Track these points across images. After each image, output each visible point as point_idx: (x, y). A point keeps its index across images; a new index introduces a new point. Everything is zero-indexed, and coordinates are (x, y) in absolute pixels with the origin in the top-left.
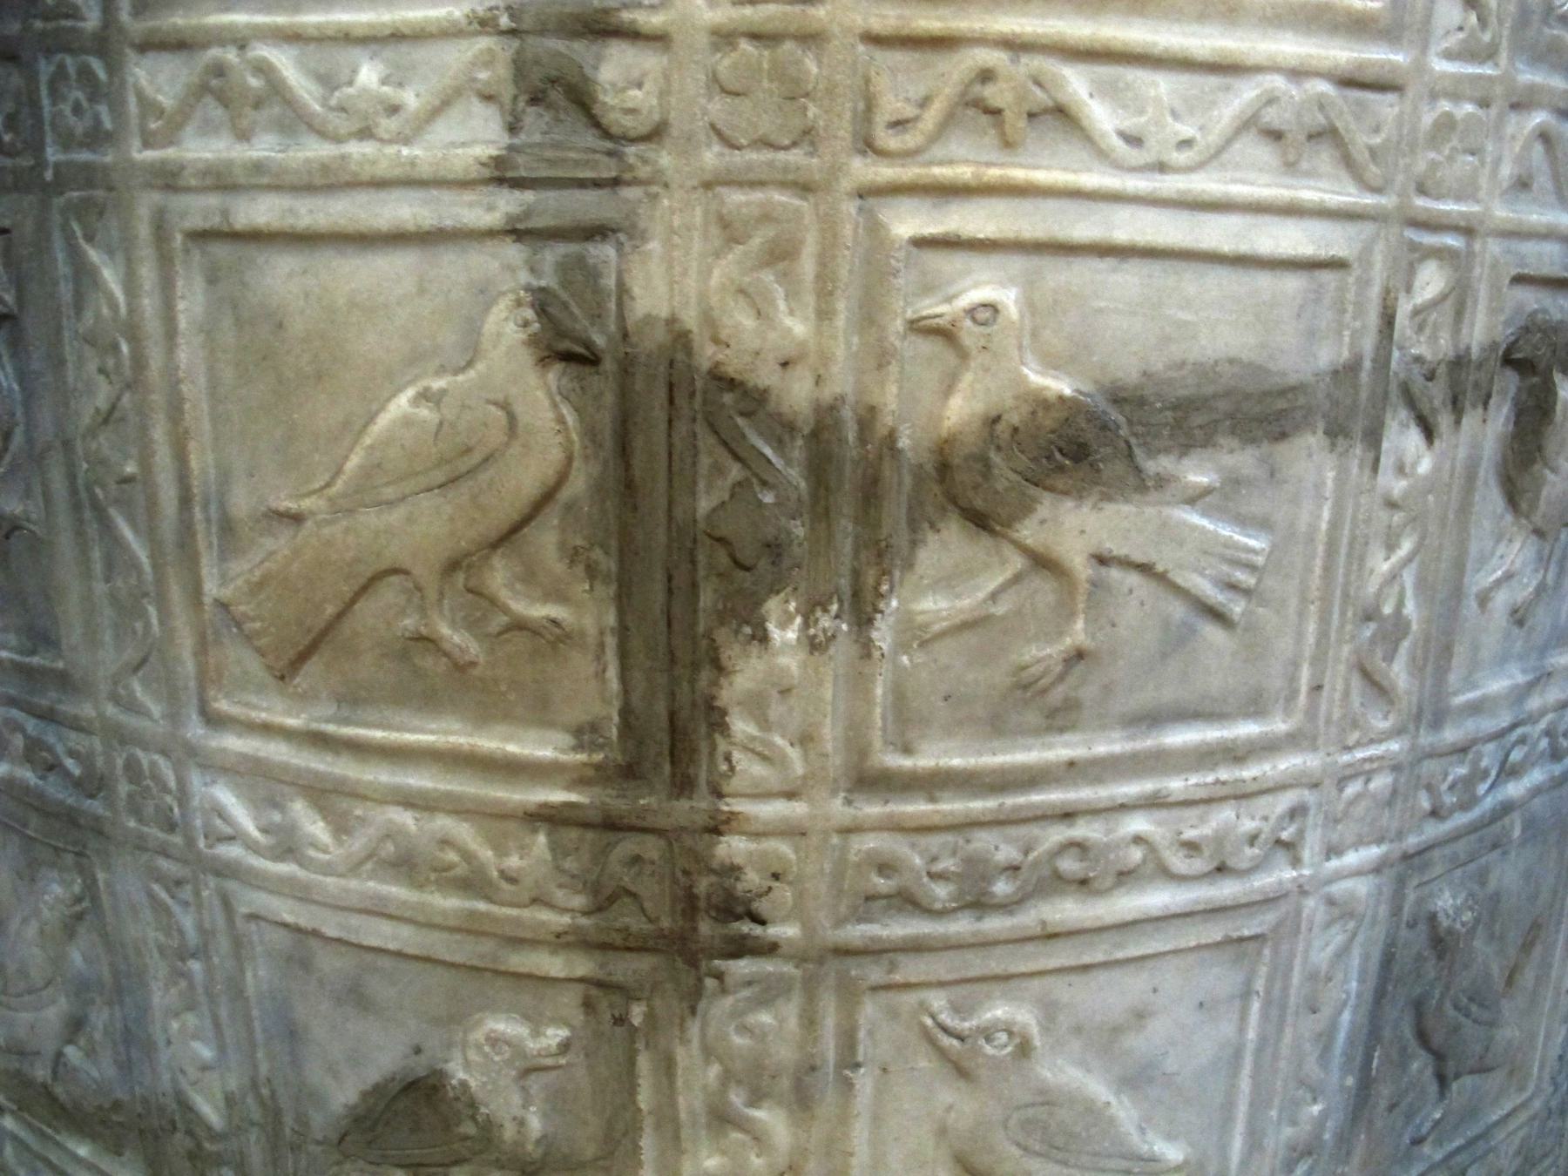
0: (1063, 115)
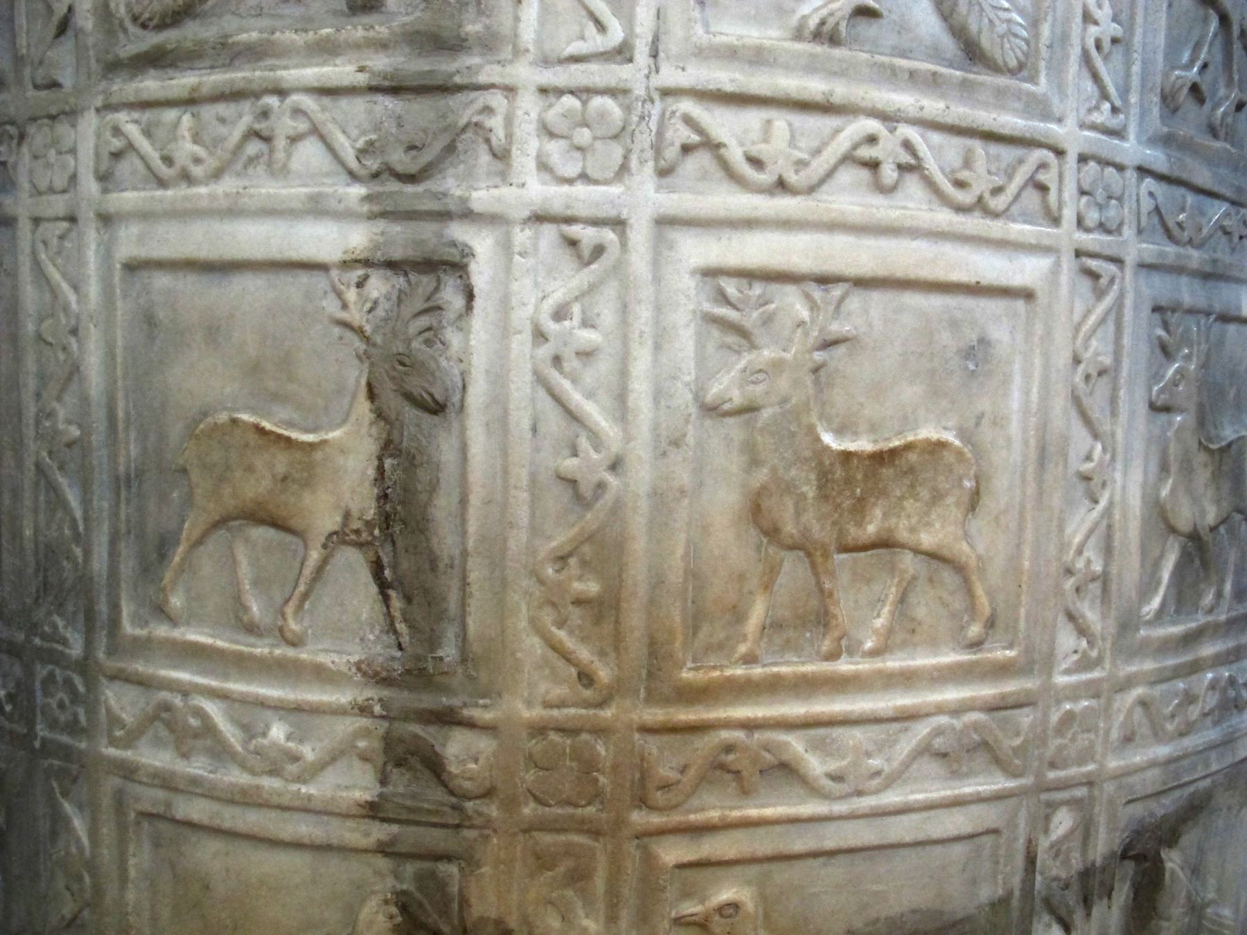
0: (787, 770)
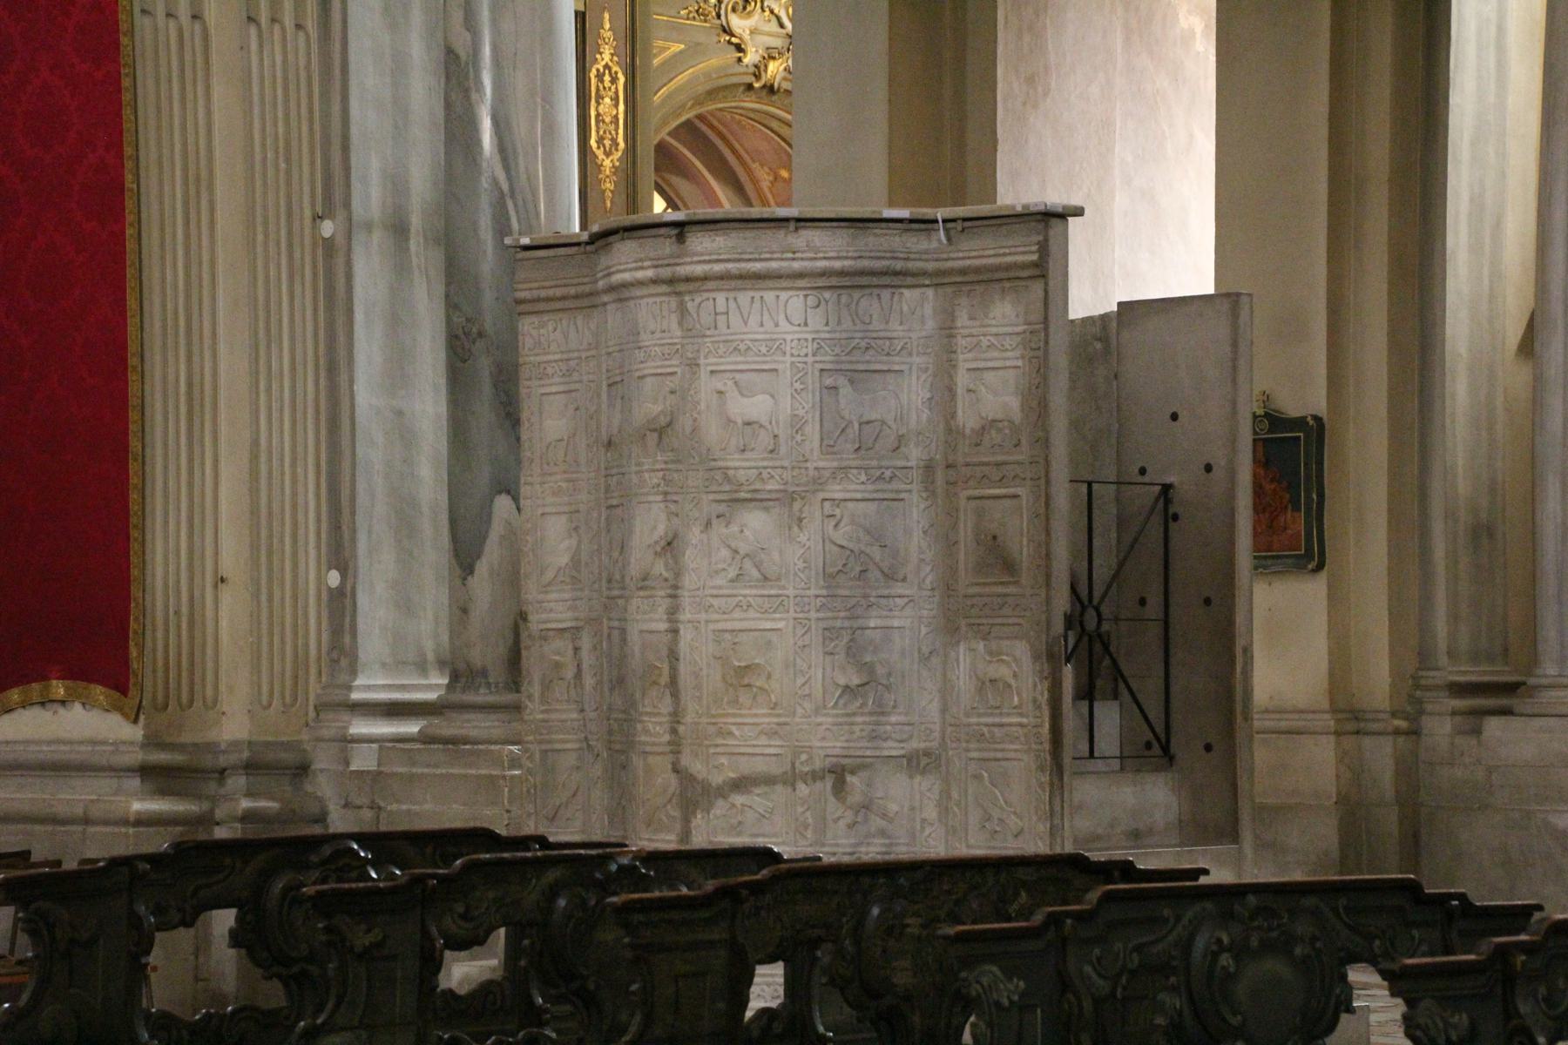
0: (730, 733)
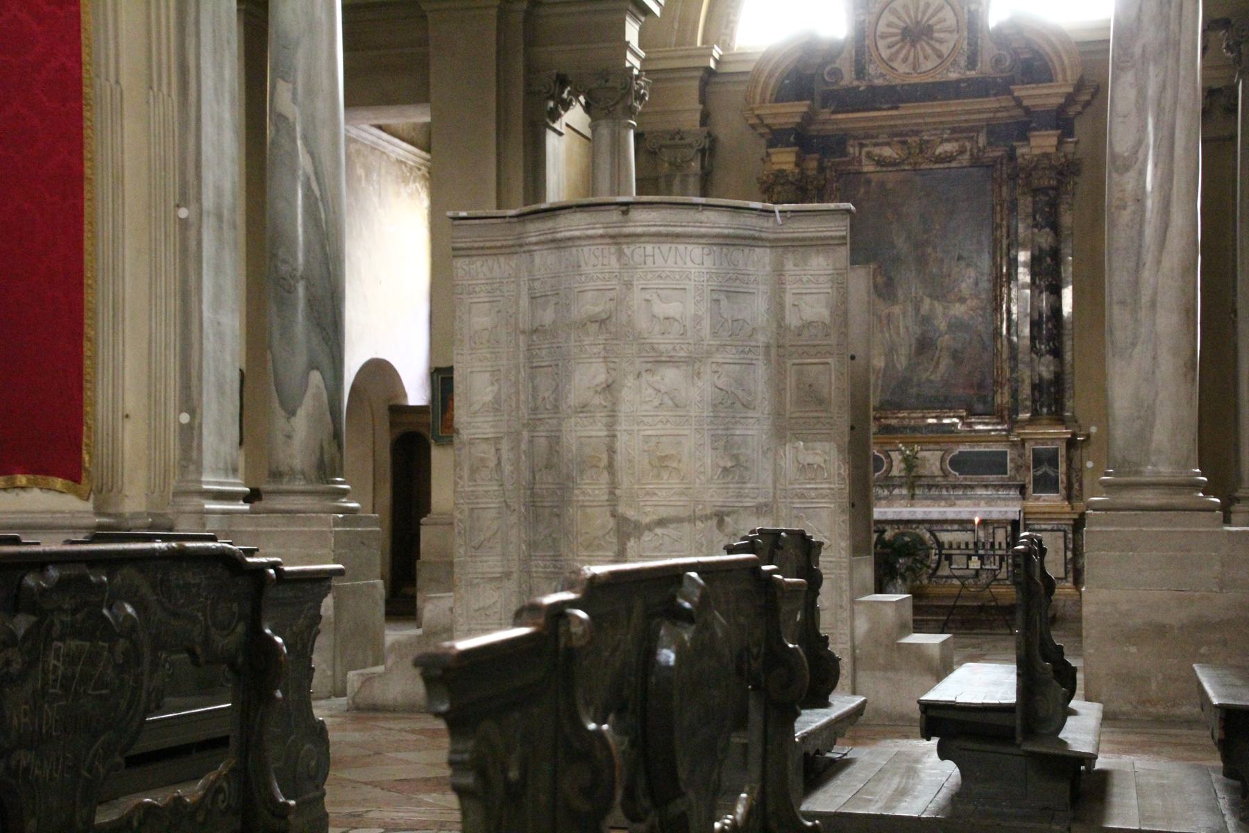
0: (655, 494)
